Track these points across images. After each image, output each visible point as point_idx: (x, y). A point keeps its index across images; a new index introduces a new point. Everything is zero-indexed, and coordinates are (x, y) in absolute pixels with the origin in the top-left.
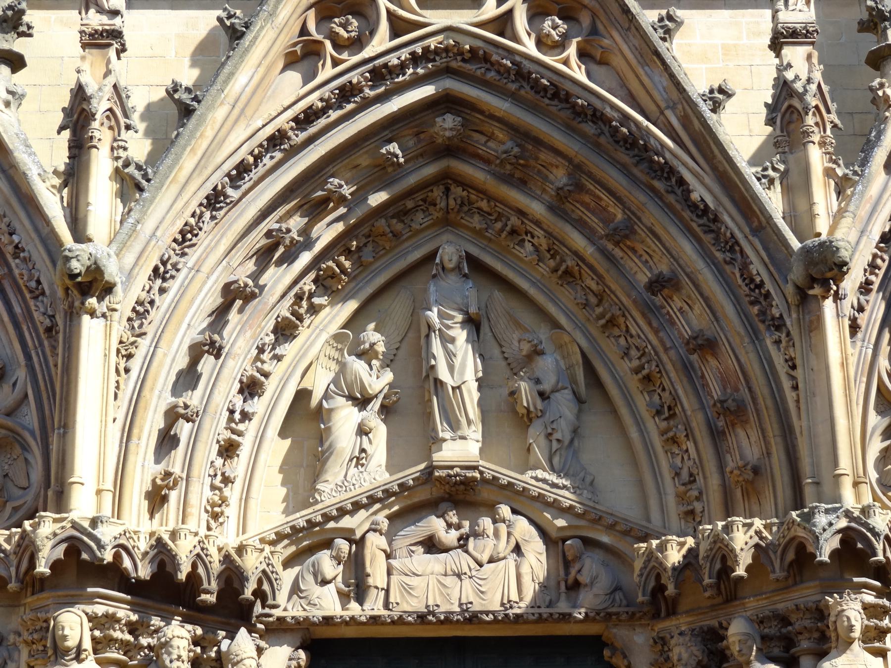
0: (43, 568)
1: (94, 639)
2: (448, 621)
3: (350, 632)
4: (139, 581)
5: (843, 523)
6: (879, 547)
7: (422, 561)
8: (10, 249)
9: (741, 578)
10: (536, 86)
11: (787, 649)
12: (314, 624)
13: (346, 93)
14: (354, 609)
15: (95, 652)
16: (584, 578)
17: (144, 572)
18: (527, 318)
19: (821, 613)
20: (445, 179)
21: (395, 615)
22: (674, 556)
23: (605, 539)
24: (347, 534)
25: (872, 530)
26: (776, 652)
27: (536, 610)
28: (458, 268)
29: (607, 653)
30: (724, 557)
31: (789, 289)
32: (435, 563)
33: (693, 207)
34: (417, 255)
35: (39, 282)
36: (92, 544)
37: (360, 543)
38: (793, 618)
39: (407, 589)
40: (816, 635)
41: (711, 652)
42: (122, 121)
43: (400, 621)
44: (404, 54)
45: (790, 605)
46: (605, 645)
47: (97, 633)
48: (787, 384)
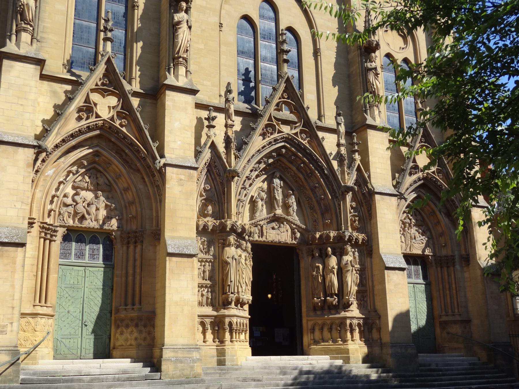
5: (349, 234)
7: (272, 231)
10: (301, 147)
13: (270, 143)
14: (261, 239)
22: (318, 236)
24: (260, 225)
30: (328, 237)
31: (340, 192)
32: (274, 232)
37: (262, 227)
39: (270, 236)
44: (280, 137)
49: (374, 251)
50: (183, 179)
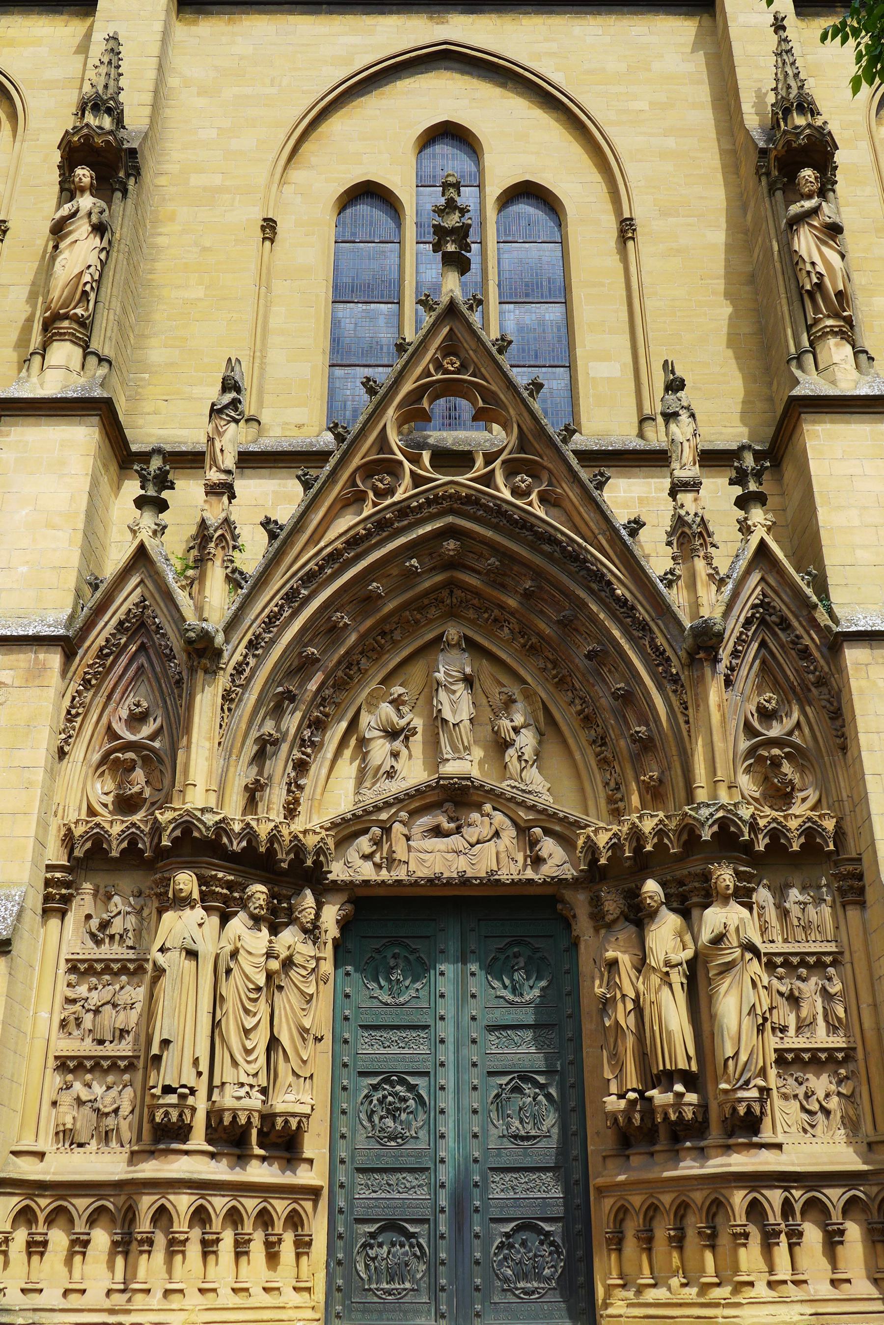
0: (166, 842)
1: (201, 892)
2: (449, 883)
3: (381, 892)
4: (233, 852)
5: (720, 814)
6: (746, 830)
8: (154, 627)
9: (649, 852)
10: (510, 519)
11: (682, 903)
12: (357, 885)
15: (202, 901)
16: (544, 854)
17: (237, 846)
18: (504, 679)
19: (706, 877)
20: (451, 585)
21: (412, 879)
23: (557, 828)
25: (740, 819)
26: (675, 905)
27: (510, 877)
28: (458, 644)
29: (559, 906)
31: (682, 654)
33: (617, 599)
34: (430, 636)
35: (171, 650)
36: (201, 826)
38: (687, 881)
40: (703, 893)
41: (630, 906)
42: (231, 543)
43: (416, 884)
45: (685, 872)
46: (558, 901)
47: (204, 888)
48: (681, 720)
49: (868, 879)
50: (8, 681)
